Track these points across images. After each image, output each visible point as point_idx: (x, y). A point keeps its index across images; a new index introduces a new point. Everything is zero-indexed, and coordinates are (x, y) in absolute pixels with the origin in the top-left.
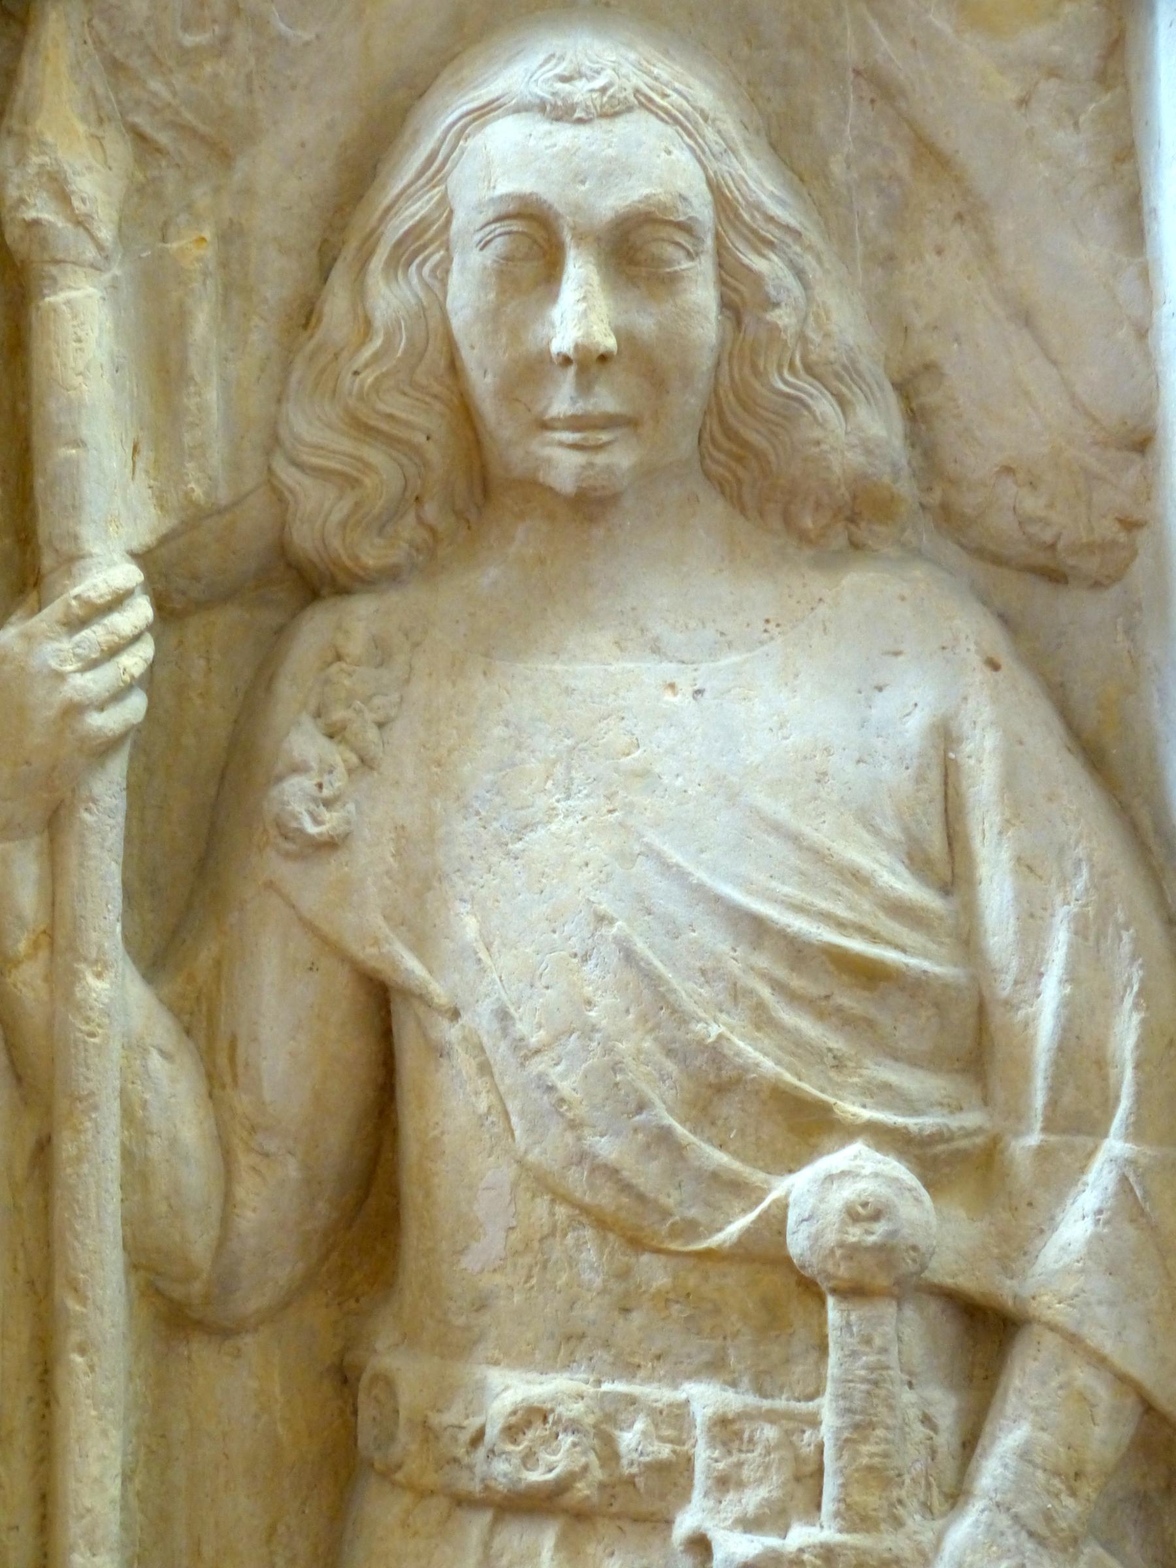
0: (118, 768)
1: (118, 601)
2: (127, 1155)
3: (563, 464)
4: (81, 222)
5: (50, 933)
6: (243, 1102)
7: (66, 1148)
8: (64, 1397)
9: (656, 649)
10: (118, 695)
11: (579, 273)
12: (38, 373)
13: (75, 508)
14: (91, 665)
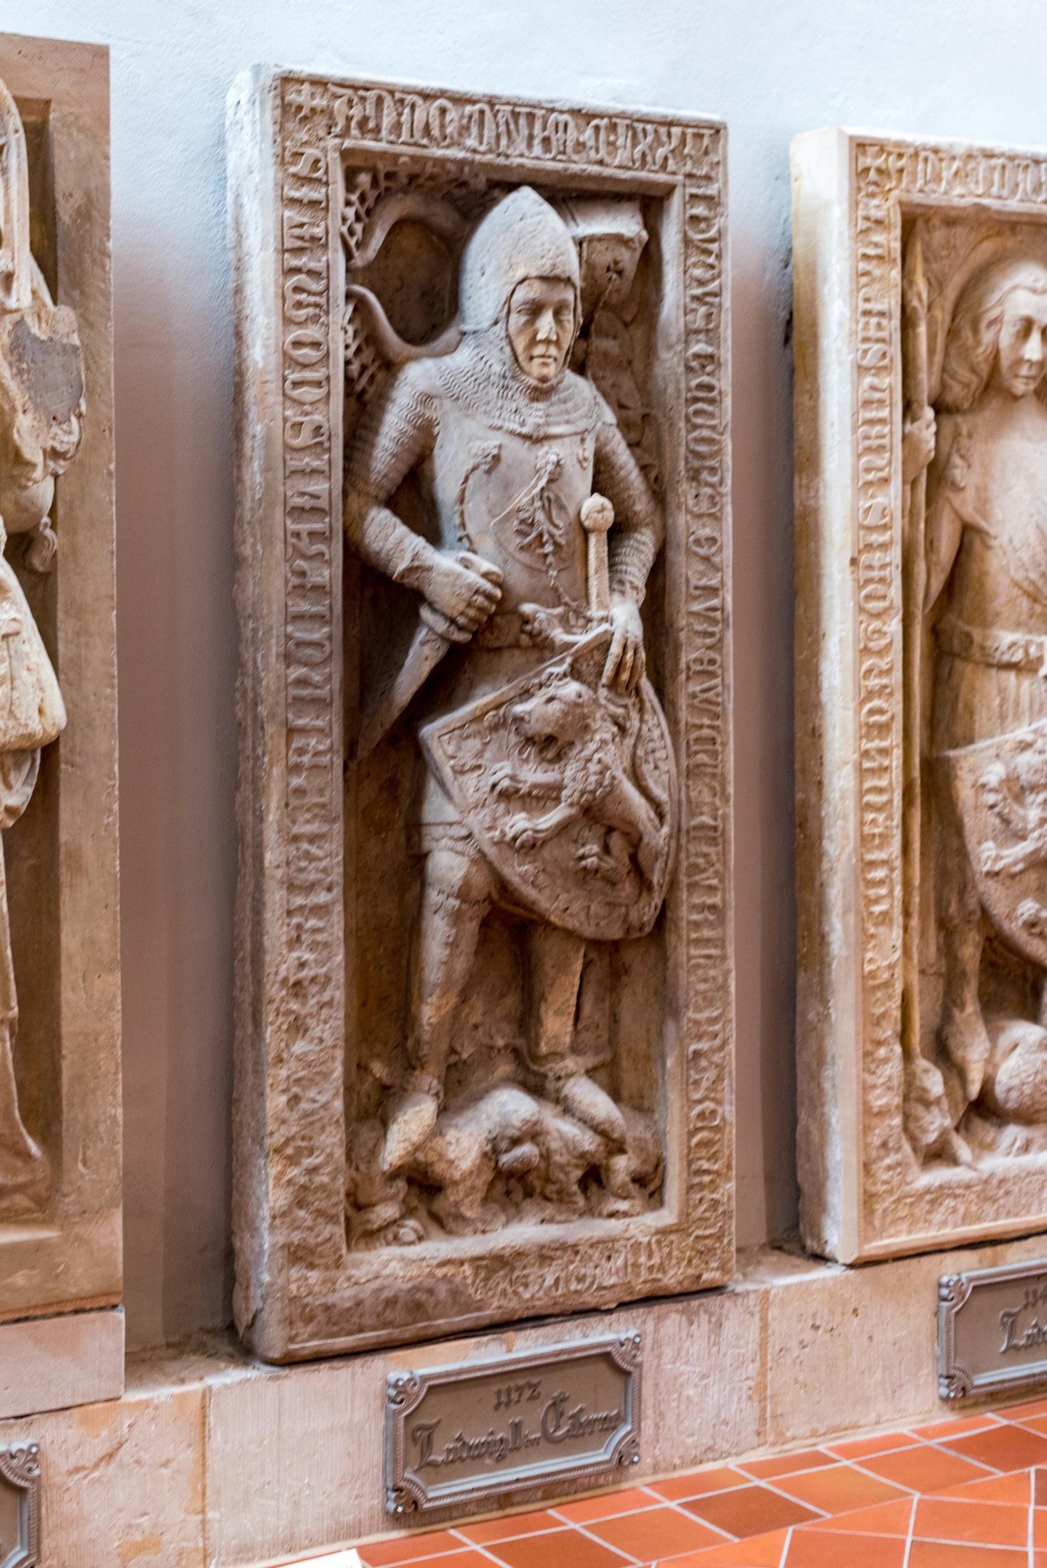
3: (1020, 387)
6: (934, 558)
9: (1029, 439)
11: (1036, 337)
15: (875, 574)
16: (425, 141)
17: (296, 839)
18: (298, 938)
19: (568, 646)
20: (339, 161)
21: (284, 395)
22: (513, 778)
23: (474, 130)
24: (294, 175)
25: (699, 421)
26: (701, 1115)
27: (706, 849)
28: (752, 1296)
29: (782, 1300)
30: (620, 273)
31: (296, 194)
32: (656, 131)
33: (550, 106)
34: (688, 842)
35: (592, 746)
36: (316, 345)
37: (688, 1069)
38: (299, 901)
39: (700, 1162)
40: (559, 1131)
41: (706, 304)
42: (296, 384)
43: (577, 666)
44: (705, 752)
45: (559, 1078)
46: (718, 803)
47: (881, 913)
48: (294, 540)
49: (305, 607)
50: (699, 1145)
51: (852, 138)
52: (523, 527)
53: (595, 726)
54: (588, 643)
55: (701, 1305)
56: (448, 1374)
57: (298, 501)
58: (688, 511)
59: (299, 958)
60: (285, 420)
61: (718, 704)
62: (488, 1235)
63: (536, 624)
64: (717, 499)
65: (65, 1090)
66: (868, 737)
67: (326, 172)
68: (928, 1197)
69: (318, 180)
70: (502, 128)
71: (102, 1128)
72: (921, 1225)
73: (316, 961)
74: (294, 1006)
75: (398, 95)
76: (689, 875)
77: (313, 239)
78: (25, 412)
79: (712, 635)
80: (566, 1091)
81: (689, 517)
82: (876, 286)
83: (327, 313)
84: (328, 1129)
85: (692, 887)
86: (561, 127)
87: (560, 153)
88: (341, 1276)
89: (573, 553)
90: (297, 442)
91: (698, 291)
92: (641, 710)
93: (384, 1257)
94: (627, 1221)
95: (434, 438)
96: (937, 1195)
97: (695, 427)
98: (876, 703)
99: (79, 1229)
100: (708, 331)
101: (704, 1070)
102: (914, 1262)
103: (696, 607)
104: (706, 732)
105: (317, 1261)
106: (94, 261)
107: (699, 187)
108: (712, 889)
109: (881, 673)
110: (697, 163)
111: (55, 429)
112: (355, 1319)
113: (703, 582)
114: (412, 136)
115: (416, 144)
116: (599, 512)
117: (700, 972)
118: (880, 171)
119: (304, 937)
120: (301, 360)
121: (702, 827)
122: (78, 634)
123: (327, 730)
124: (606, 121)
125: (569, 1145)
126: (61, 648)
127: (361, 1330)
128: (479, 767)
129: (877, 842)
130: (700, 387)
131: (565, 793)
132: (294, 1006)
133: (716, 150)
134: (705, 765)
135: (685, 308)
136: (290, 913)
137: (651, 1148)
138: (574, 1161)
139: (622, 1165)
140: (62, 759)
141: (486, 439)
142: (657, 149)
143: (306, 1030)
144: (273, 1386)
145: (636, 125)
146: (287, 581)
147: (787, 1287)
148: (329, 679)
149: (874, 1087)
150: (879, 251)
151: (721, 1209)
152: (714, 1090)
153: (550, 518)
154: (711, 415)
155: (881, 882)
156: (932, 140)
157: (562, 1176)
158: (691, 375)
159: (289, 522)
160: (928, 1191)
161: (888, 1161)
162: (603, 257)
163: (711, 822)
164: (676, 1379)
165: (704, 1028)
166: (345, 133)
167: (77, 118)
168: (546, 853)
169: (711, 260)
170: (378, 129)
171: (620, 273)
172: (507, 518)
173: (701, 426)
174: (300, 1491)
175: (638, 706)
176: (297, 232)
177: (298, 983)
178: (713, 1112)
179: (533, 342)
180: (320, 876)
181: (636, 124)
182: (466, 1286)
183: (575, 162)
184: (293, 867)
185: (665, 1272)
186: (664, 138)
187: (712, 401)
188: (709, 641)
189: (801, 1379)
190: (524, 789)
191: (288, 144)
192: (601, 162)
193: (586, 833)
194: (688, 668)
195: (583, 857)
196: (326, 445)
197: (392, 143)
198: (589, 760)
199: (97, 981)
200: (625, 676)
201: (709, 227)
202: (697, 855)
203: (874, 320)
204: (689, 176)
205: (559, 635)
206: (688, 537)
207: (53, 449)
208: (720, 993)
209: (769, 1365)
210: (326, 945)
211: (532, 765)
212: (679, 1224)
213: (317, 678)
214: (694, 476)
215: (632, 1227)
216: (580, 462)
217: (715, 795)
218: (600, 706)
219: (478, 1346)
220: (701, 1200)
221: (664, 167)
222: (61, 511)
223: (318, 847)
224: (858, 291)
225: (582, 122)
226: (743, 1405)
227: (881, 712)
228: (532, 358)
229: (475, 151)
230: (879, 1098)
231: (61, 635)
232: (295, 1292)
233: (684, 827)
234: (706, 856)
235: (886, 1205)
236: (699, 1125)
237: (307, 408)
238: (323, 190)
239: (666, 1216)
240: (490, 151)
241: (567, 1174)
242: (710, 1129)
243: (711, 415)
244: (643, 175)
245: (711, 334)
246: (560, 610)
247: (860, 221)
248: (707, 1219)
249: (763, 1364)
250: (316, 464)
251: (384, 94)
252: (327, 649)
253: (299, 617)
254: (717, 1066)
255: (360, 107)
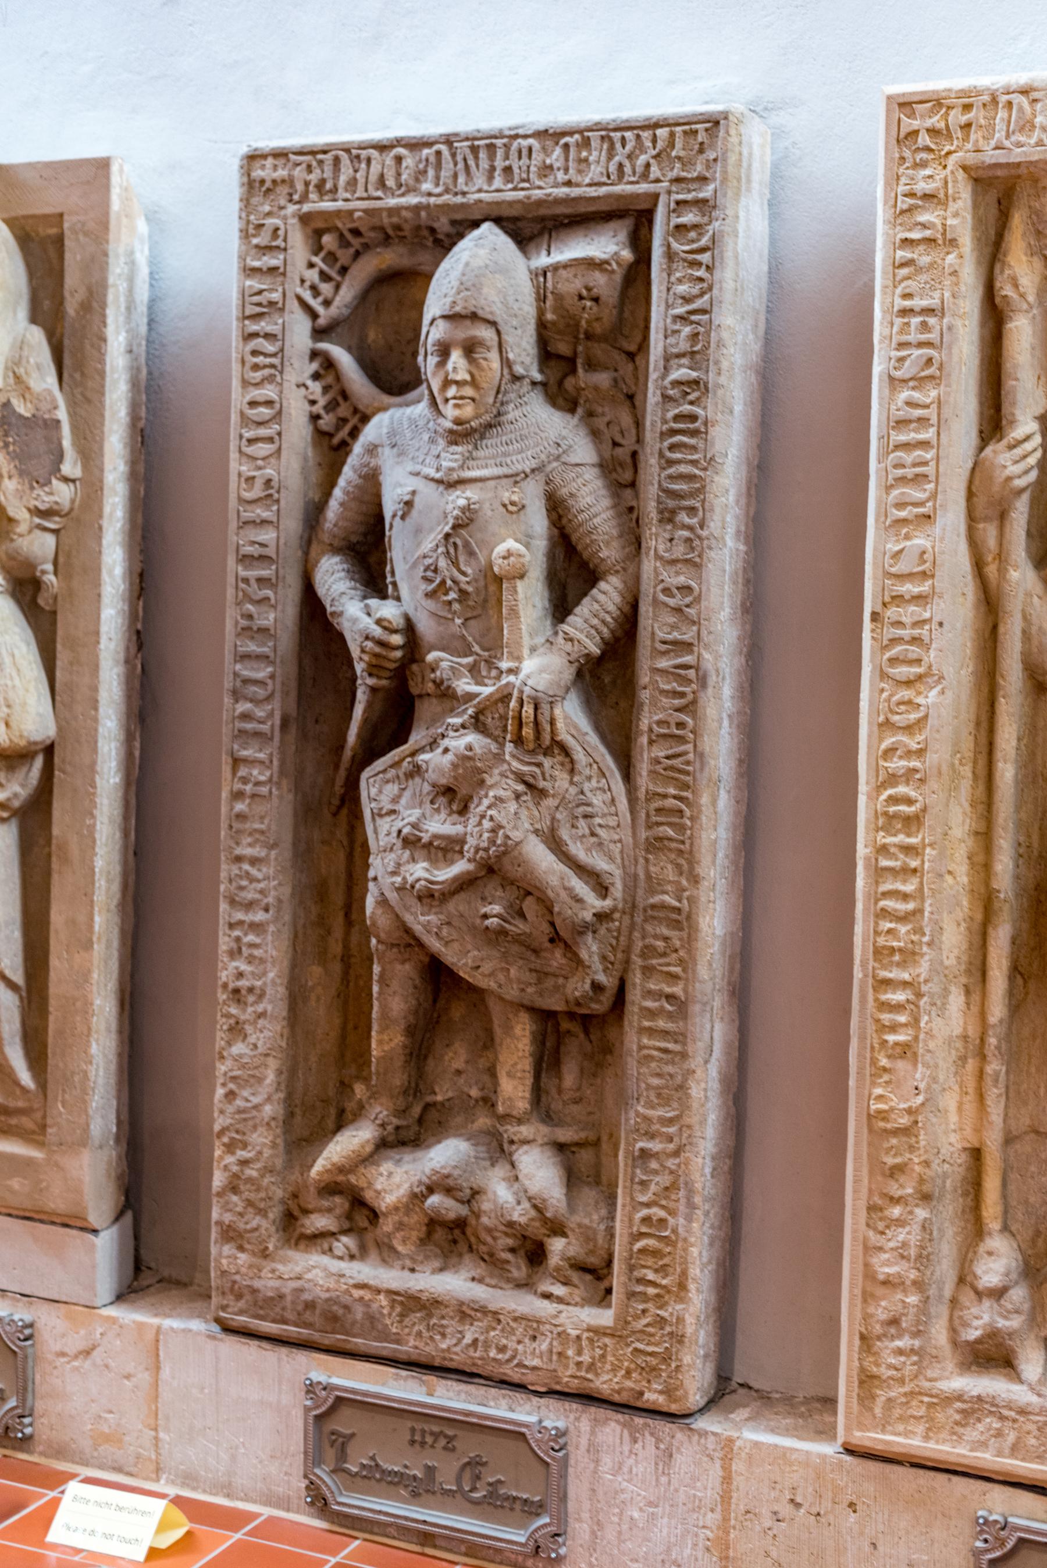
0: (1025, 497)
1: (1027, 438)
2: (1024, 632)
4: (1022, 296)
5: (999, 555)
7: (1001, 629)
8: (998, 712)
10: (1026, 472)
12: (1005, 353)
13: (1014, 404)
14: (1016, 462)
15: (906, 633)
16: (379, 193)
17: (239, 859)
18: (240, 949)
19: (470, 697)
20: (298, 226)
21: (240, 451)
22: (415, 826)
23: (431, 173)
24: (257, 246)
25: (678, 456)
26: (646, 1220)
27: (666, 932)
28: (711, 1438)
29: (750, 1456)
30: (596, 300)
31: (256, 264)
32: (638, 136)
33: (512, 133)
34: (645, 920)
35: (486, 802)
36: (269, 403)
37: (634, 1167)
38: (240, 916)
39: (645, 1271)
40: (495, 1193)
41: (692, 323)
42: (251, 441)
43: (482, 718)
44: (670, 824)
45: (512, 1142)
46: (684, 882)
47: (896, 1044)
48: (242, 585)
49: (252, 647)
50: (642, 1251)
51: (889, 98)
52: (429, 574)
53: (489, 781)
54: (491, 694)
55: (646, 1425)
56: (366, 1394)
57: (249, 549)
58: (658, 557)
59: (237, 968)
60: (240, 475)
61: (688, 773)
62: (417, 1275)
63: (438, 673)
64: (697, 542)
65: (50, 1040)
66: (888, 829)
67: (285, 240)
68: (958, 1405)
69: (278, 247)
70: (461, 165)
71: (76, 1078)
72: (944, 1435)
73: (253, 973)
74: (233, 1010)
75: (354, 152)
76: (643, 955)
77: (271, 304)
78: (10, 477)
79: (682, 695)
80: (515, 1157)
81: (658, 564)
82: (924, 277)
83: (281, 372)
84: (260, 1129)
85: (648, 971)
86: (525, 152)
87: (523, 181)
88: (268, 1265)
89: (485, 601)
90: (248, 495)
91: (680, 310)
92: (572, 771)
93: (311, 1263)
94: (562, 1307)
95: (380, 485)
96: (975, 1408)
97: (671, 463)
98: (902, 789)
99: (56, 1157)
100: (693, 353)
101: (656, 1172)
102: (942, 1477)
103: (664, 663)
104: (671, 802)
105: (247, 1246)
106: (92, 346)
107: (689, 191)
108: (674, 977)
109: (909, 754)
110: (686, 163)
111: (38, 491)
112: (278, 1310)
113: (676, 635)
114: (366, 190)
115: (369, 198)
116: (504, 558)
117: (653, 1065)
118: (933, 132)
119: (244, 949)
120: (256, 419)
121: (663, 906)
122: (71, 664)
123: (267, 762)
124: (577, 136)
125: (500, 1211)
126: (58, 674)
127: (284, 1321)
128: (394, 812)
129: (897, 958)
130: (677, 418)
131: (466, 848)
132: (233, 1010)
133: (713, 146)
134: (670, 839)
135: (666, 330)
136: (231, 926)
137: (600, 1241)
138: (503, 1228)
139: (557, 1246)
140: (56, 767)
141: (406, 485)
142: (637, 157)
143: (246, 1036)
144: (210, 1345)
145: (612, 134)
146: (237, 623)
147: (756, 1444)
148: (271, 715)
149: (880, 1249)
150: (928, 233)
151: (668, 1329)
152: (667, 1198)
153: (455, 563)
154: (694, 448)
155: (898, 1008)
156: (1022, 78)
157: (489, 1240)
158: (668, 406)
159: (240, 568)
160: (960, 1397)
161: (899, 1343)
162: (571, 285)
163: (677, 904)
164: (616, 1492)
165: (656, 1127)
166: (304, 198)
167: (84, 224)
168: (451, 906)
169: (701, 273)
170: (335, 190)
171: (596, 300)
172: (414, 565)
173: (679, 462)
174: (237, 1448)
175: (568, 766)
176: (256, 299)
177: (237, 991)
178: (662, 1221)
179: (447, 383)
180: (257, 896)
181: (609, 133)
182: (381, 1313)
183: (540, 188)
184: (234, 884)
185: (597, 1375)
186: (648, 144)
187: (694, 433)
188: (677, 702)
189: (774, 1554)
190: (426, 838)
191: (252, 217)
192: (569, 183)
193: (499, 893)
194: (651, 730)
195: (485, 916)
196: (276, 496)
197: (346, 200)
198: (483, 817)
199: (77, 955)
200: (528, 732)
201: (701, 235)
202: (656, 937)
203: (916, 321)
204: (678, 180)
205: (464, 685)
206: (655, 587)
207: (36, 507)
208: (680, 1094)
209: (733, 1522)
210: (262, 961)
211: (443, 815)
212: (614, 1328)
213: (260, 713)
214: (668, 517)
215: (564, 1315)
216: (505, 506)
217: (681, 874)
218: (504, 761)
219: (397, 1377)
220: (644, 1311)
221: (645, 176)
222: (61, 560)
223: (259, 870)
224: (895, 287)
225: (549, 143)
226: (700, 1555)
227: (910, 802)
228: (447, 400)
229: (430, 194)
230: (887, 1263)
231: (59, 663)
232: (225, 1268)
233: (641, 904)
234: (666, 939)
235: (892, 1394)
236: (644, 1230)
237: (260, 463)
238: (281, 257)
239: (605, 1317)
240: (447, 191)
241: (494, 1239)
242: (661, 1238)
243: (694, 448)
244: (618, 189)
245: (698, 357)
246: (470, 660)
247: (900, 198)
248: (652, 1335)
249: (726, 1519)
250: (266, 515)
251: (341, 153)
252: (270, 688)
253: (245, 657)
254: (672, 1172)
255: (318, 171)
